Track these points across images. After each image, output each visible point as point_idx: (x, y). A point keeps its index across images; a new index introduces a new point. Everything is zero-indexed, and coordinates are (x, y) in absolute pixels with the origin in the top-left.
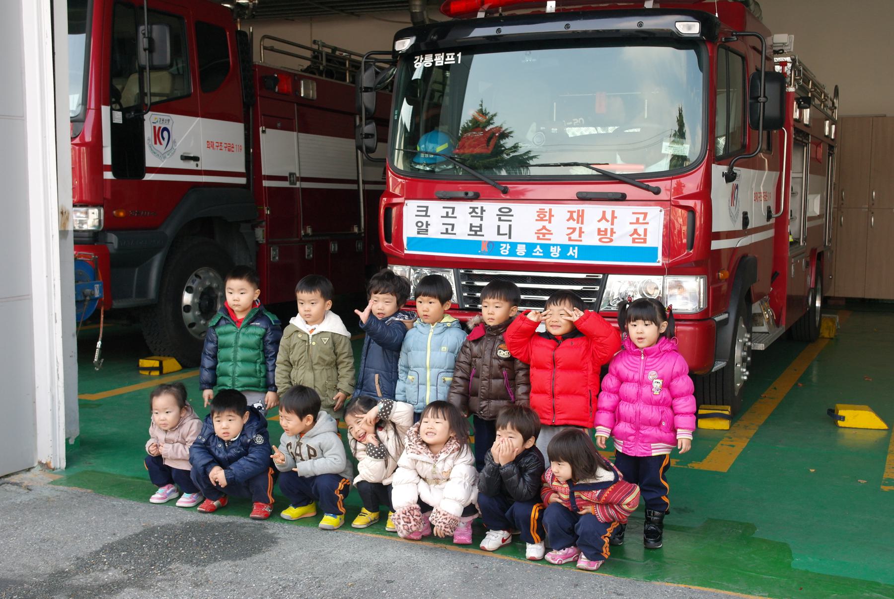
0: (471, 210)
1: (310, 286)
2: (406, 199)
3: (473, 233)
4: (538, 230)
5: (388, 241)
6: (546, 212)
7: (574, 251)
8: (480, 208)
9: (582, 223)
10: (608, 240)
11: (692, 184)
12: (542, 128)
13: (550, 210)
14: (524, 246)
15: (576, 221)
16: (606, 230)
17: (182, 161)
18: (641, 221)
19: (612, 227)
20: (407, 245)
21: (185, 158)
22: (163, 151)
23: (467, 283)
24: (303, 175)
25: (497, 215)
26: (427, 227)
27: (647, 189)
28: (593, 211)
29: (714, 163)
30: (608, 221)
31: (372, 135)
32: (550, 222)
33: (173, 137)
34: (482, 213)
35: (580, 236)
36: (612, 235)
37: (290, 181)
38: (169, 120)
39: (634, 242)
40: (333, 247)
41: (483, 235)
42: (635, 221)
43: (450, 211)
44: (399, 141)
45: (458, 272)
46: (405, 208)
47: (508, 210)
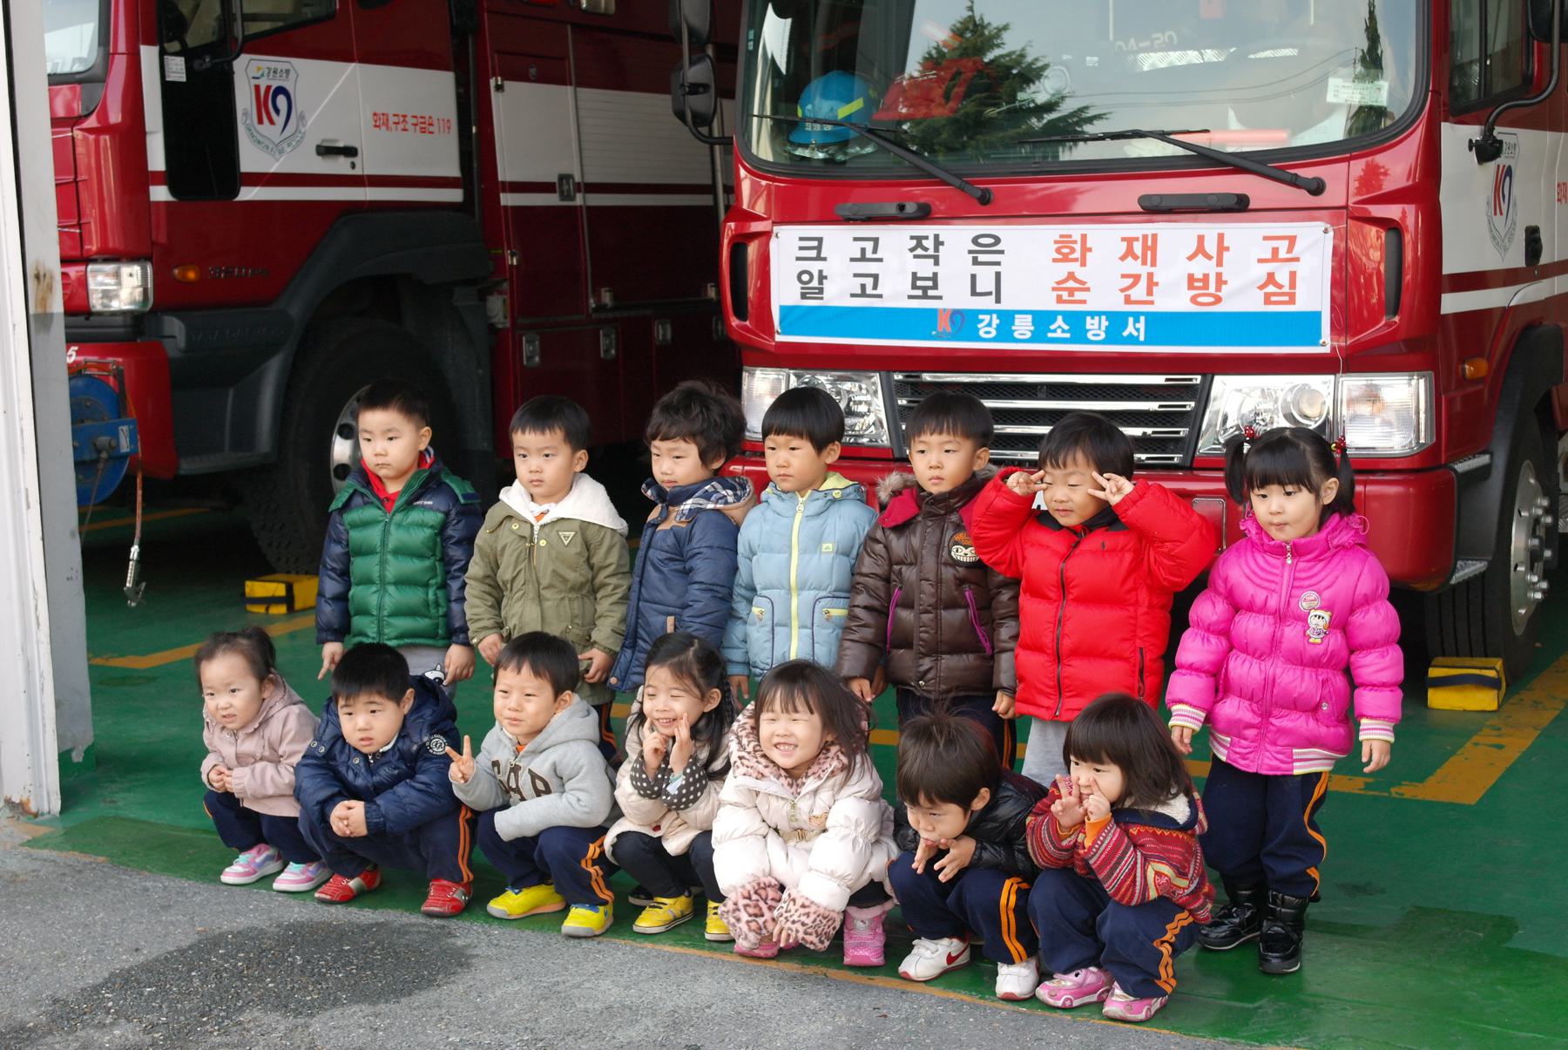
0: (914, 242)
1: (541, 418)
2: (774, 223)
3: (919, 293)
4: (1058, 283)
5: (741, 313)
6: (1075, 242)
7: (1137, 326)
8: (931, 238)
9: (1154, 264)
10: (1211, 299)
11: (1399, 165)
12: (1065, 57)
13: (1084, 237)
14: (1029, 317)
15: (1140, 260)
16: (1206, 277)
17: (320, 158)
18: (1282, 254)
19: (1219, 270)
20: (781, 322)
21: (326, 151)
23: (909, 402)
24: (590, 179)
25: (970, 252)
26: (821, 282)
27: (1295, 182)
28: (1176, 236)
29: (1446, 121)
30: (1209, 257)
31: (706, 87)
32: (1083, 264)
33: (298, 106)
34: (936, 250)
35: (1150, 293)
36: (1218, 289)
37: (562, 193)
38: (288, 71)
39: (1267, 301)
40: (661, 332)
41: (940, 298)
42: (1269, 256)
43: (869, 246)
44: (761, 97)
45: (889, 379)
46: (773, 244)
47: (991, 241)
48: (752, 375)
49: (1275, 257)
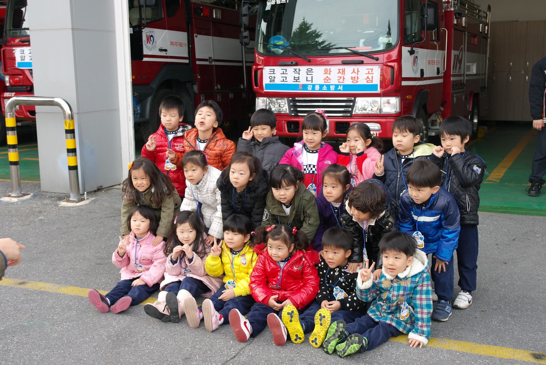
0: (294, 70)
2: (264, 66)
3: (295, 81)
5: (256, 86)
8: (298, 69)
9: (344, 74)
11: (394, 54)
12: (326, 32)
13: (330, 69)
14: (319, 86)
16: (355, 77)
18: (370, 72)
19: (357, 76)
20: (265, 87)
21: (161, 50)
22: (151, 47)
24: (216, 58)
27: (373, 58)
28: (349, 69)
29: (403, 46)
30: (355, 73)
31: (247, 37)
32: (330, 74)
34: (299, 72)
35: (343, 80)
36: (357, 80)
39: (367, 82)
42: (368, 73)
43: (285, 71)
44: (260, 40)
45: (289, 99)
46: (264, 71)
47: (311, 70)
48: (258, 99)
49: (369, 73)
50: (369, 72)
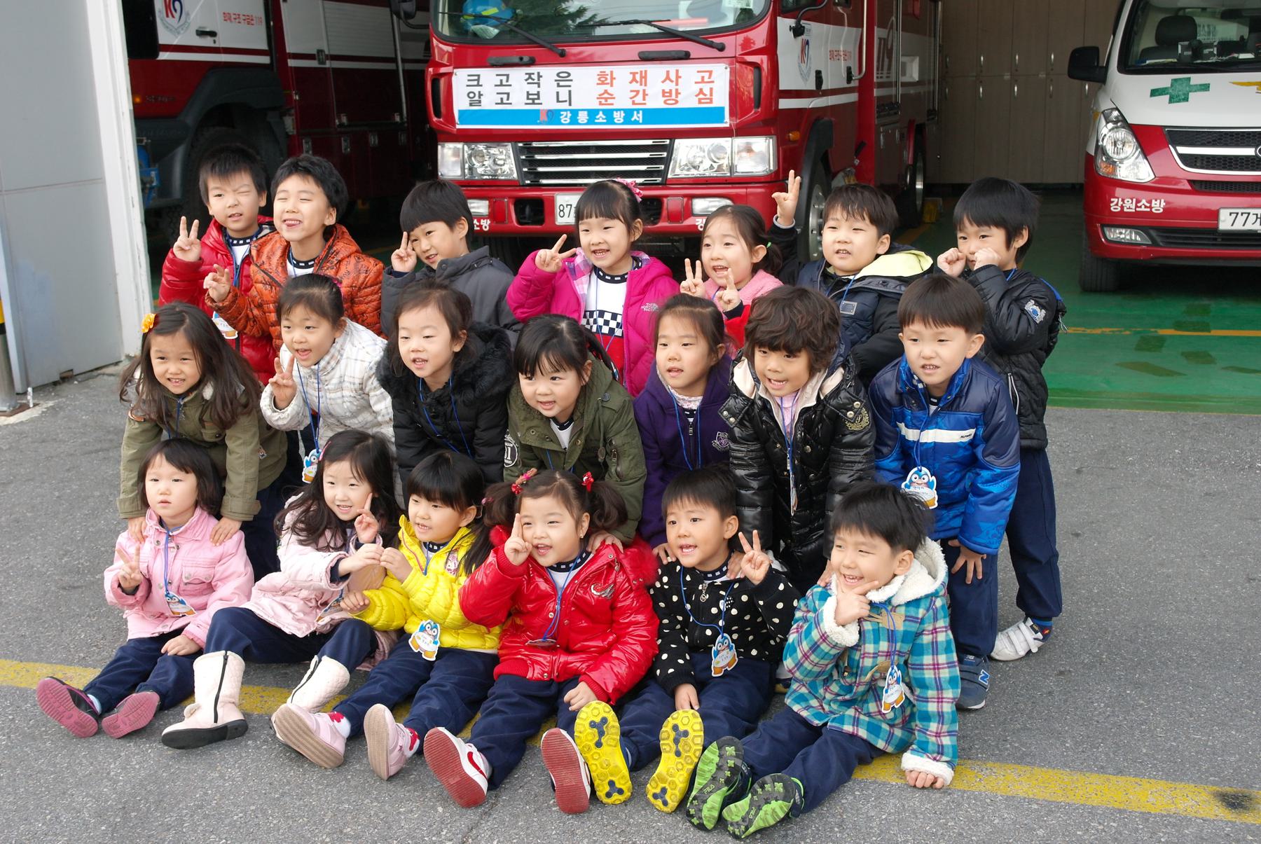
0: (527, 76)
2: (454, 68)
3: (531, 101)
5: (438, 114)
9: (646, 85)
10: (673, 102)
11: (759, 36)
13: (612, 72)
14: (586, 112)
16: (671, 90)
17: (198, 37)
18: (706, 79)
20: (459, 119)
21: (201, 33)
22: (176, 26)
27: (711, 45)
28: (656, 71)
30: (672, 81)
32: (612, 85)
34: (539, 80)
35: (644, 99)
36: (677, 97)
37: (319, 60)
39: (700, 102)
41: (541, 104)
42: (700, 80)
43: (504, 78)
45: (516, 146)
46: (454, 78)
47: (566, 75)
48: (443, 147)
49: (703, 81)
50: (703, 78)
